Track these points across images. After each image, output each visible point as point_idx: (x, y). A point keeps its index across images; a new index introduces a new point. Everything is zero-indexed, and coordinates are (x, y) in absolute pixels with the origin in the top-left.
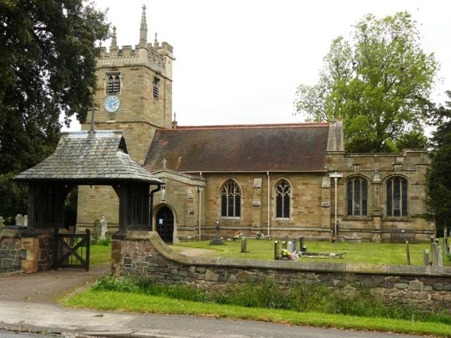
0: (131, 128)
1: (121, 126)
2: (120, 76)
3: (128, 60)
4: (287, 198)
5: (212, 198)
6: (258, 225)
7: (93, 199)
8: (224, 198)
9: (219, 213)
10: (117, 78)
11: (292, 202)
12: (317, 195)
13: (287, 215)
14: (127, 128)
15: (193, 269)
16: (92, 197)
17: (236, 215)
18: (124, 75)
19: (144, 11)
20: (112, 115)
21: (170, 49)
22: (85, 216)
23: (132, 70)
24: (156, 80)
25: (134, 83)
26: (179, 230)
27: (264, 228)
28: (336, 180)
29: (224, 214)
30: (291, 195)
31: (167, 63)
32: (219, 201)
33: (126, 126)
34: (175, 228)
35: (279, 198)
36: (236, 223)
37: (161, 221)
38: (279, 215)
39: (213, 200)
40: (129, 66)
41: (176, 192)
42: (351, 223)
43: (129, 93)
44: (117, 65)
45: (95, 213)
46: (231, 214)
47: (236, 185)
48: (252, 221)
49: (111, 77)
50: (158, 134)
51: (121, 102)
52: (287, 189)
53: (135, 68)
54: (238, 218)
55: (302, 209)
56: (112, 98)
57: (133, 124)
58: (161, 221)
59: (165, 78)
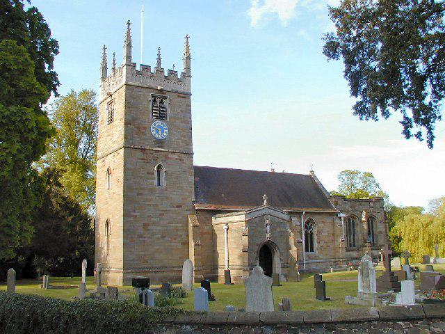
1: (170, 156)
4: (311, 234)
7: (141, 239)
10: (161, 102)
11: (315, 238)
12: (331, 232)
13: (312, 250)
16: (140, 236)
18: (170, 100)
20: (160, 143)
22: (134, 260)
23: (179, 96)
28: (342, 219)
30: (315, 232)
33: (175, 156)
35: (306, 235)
38: (307, 250)
40: (177, 92)
42: (351, 253)
44: (165, 89)
45: (145, 255)
49: (155, 100)
51: (169, 129)
52: (311, 227)
53: (182, 95)
55: (322, 243)
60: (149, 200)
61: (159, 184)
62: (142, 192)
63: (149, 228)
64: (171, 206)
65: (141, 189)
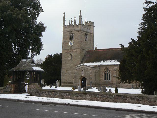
0: (77, 51)
1: (74, 50)
2: (73, 34)
3: (76, 28)
5: (101, 74)
6: (115, 83)
8: (105, 74)
9: (104, 79)
10: (73, 35)
14: (76, 51)
15: (43, 92)
16: (66, 74)
17: (107, 80)
19: (81, 12)
20: (71, 47)
21: (93, 23)
24: (86, 35)
25: (78, 36)
26: (88, 84)
27: (118, 84)
29: (105, 79)
31: (91, 28)
32: (104, 75)
33: (75, 50)
34: (86, 84)
36: (109, 82)
37: (83, 82)
39: (102, 75)
40: (76, 30)
41: (87, 72)
43: (76, 39)
46: (107, 80)
47: (109, 70)
48: (113, 82)
50: (87, 53)
54: (110, 81)
56: (71, 41)
57: (77, 50)
58: (83, 82)
59: (90, 33)
60: (68, 64)
61: (71, 59)
62: (66, 62)
63: (68, 71)
64: (74, 65)
65: (66, 61)
